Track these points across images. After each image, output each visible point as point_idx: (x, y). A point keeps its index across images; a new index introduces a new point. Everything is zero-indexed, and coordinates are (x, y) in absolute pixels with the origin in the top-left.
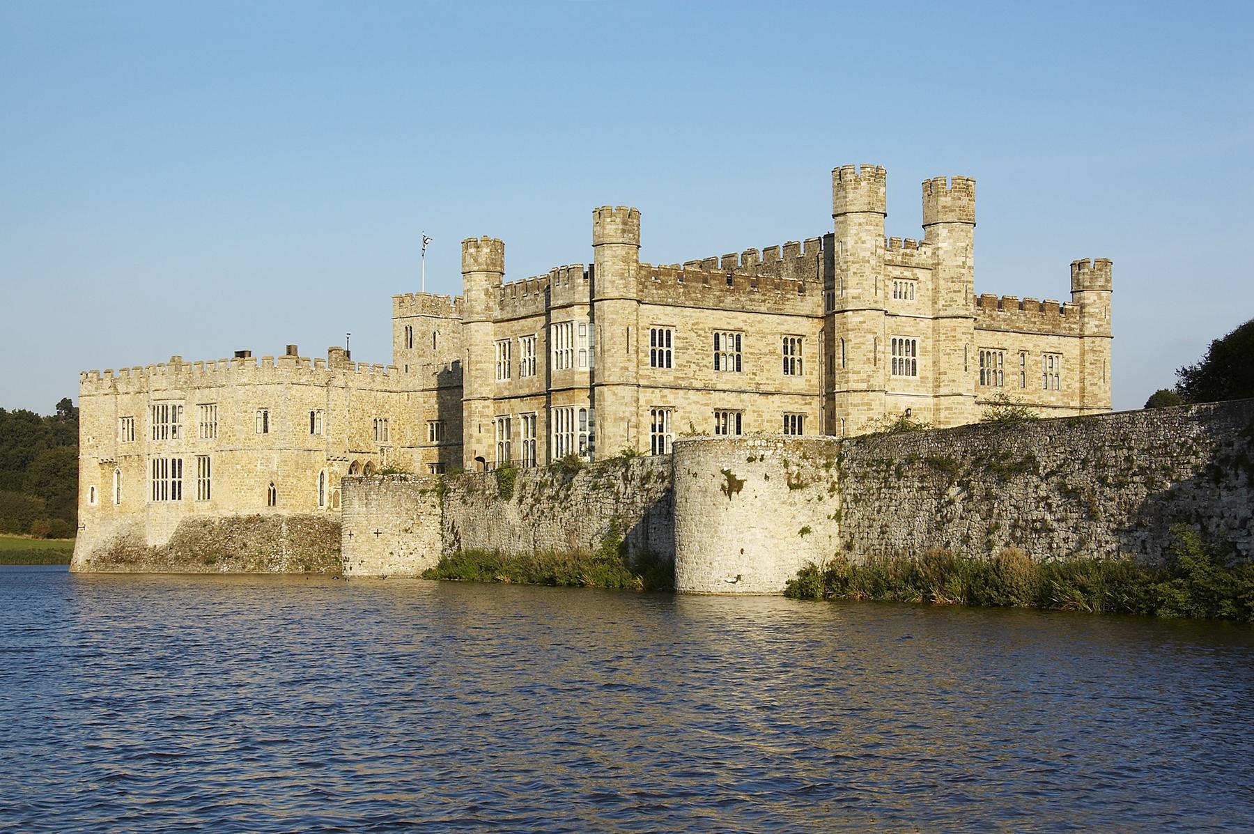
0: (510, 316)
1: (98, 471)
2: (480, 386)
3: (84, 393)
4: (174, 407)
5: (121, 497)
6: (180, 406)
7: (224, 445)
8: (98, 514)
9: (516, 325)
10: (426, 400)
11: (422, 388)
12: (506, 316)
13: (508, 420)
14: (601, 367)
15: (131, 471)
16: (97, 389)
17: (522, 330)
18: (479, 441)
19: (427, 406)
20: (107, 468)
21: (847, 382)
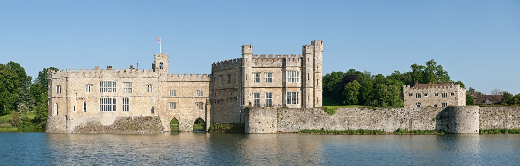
0: (260, 66)
1: (76, 101)
2: (251, 84)
3: (71, 76)
4: (113, 83)
5: (87, 110)
6: (115, 82)
7: (135, 95)
8: (77, 115)
9: (263, 69)
10: (168, 84)
11: (167, 80)
12: (257, 66)
13: (259, 94)
14: (309, 83)
15: (91, 102)
16: (76, 75)
17: (266, 70)
18: (250, 98)
19: (169, 86)
20: (79, 100)
21: (319, 89)
